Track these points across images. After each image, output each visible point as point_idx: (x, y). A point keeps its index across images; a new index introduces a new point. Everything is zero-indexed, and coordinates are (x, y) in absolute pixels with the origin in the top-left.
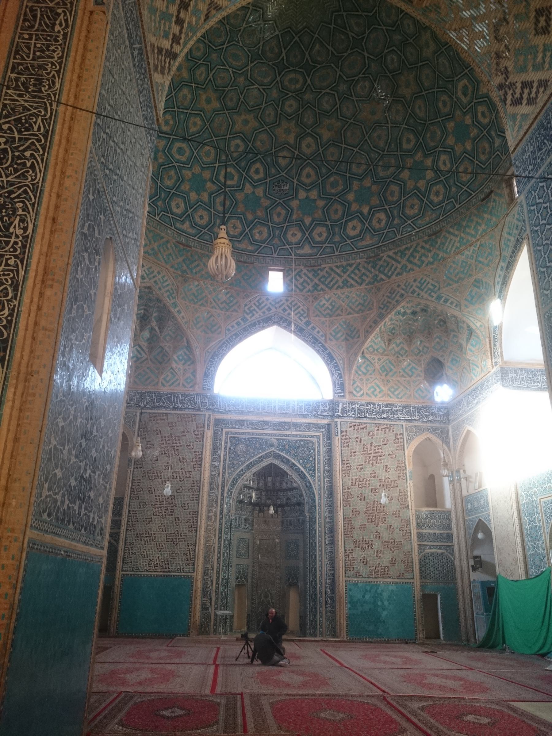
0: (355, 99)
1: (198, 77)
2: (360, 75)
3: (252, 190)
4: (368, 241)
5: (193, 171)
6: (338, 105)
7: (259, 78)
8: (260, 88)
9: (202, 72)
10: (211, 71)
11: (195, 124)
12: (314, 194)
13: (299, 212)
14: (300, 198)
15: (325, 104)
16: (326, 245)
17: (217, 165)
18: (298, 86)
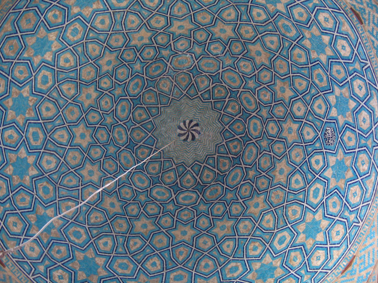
0: (256, 72)
1: (237, 212)
2: (237, 71)
3: (330, 169)
4: (346, 28)
5: (301, 231)
6: (265, 86)
7: (253, 158)
8: (259, 157)
9: (236, 208)
10: (238, 200)
11: (268, 221)
12: (332, 99)
13: (347, 116)
14: (336, 115)
15: (267, 98)
16: (366, 79)
17: (305, 205)
18: (259, 123)
